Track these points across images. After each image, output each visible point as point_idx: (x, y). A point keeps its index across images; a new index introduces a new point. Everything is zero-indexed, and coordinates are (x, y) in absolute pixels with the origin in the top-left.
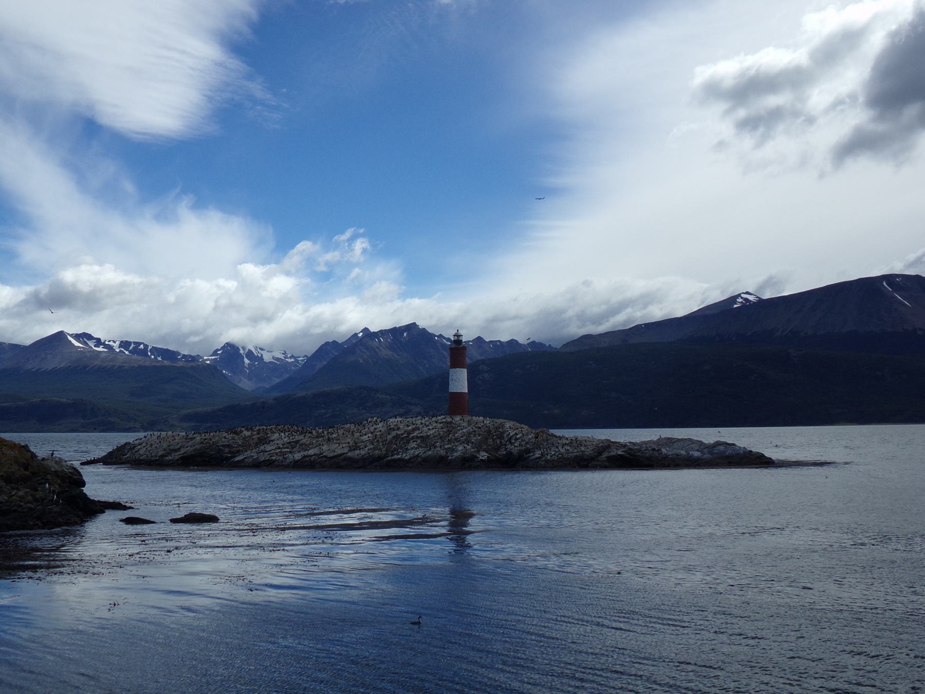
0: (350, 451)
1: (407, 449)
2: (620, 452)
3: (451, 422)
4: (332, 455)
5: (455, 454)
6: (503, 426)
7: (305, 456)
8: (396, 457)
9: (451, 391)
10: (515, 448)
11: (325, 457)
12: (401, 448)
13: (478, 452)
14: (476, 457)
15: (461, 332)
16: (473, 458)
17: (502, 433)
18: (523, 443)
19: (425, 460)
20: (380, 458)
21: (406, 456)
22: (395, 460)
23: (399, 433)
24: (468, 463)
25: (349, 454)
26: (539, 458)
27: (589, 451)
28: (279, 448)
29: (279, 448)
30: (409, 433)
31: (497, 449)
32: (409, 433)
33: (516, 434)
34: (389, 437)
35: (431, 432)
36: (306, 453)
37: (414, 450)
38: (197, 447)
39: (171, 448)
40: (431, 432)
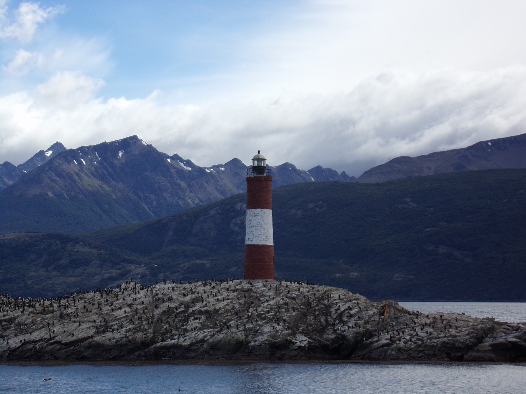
0: (98, 333)
1: (186, 331)
2: (511, 338)
3: (250, 290)
4: (70, 339)
5: (261, 339)
7: (25, 343)
8: (169, 342)
9: (248, 242)
10: (349, 330)
11: (59, 342)
12: (177, 329)
13: (294, 334)
14: (291, 342)
15: (263, 155)
16: (287, 344)
17: (328, 307)
18: (361, 322)
19: (215, 347)
20: (145, 344)
21: (185, 341)
22: (168, 348)
23: (172, 305)
24: (279, 353)
25: (97, 338)
26: (387, 345)
27: (463, 336)
30: (187, 307)
31: (322, 330)
33: (350, 308)
34: (157, 312)
35: (221, 305)
36: (27, 337)
40: (221, 305)
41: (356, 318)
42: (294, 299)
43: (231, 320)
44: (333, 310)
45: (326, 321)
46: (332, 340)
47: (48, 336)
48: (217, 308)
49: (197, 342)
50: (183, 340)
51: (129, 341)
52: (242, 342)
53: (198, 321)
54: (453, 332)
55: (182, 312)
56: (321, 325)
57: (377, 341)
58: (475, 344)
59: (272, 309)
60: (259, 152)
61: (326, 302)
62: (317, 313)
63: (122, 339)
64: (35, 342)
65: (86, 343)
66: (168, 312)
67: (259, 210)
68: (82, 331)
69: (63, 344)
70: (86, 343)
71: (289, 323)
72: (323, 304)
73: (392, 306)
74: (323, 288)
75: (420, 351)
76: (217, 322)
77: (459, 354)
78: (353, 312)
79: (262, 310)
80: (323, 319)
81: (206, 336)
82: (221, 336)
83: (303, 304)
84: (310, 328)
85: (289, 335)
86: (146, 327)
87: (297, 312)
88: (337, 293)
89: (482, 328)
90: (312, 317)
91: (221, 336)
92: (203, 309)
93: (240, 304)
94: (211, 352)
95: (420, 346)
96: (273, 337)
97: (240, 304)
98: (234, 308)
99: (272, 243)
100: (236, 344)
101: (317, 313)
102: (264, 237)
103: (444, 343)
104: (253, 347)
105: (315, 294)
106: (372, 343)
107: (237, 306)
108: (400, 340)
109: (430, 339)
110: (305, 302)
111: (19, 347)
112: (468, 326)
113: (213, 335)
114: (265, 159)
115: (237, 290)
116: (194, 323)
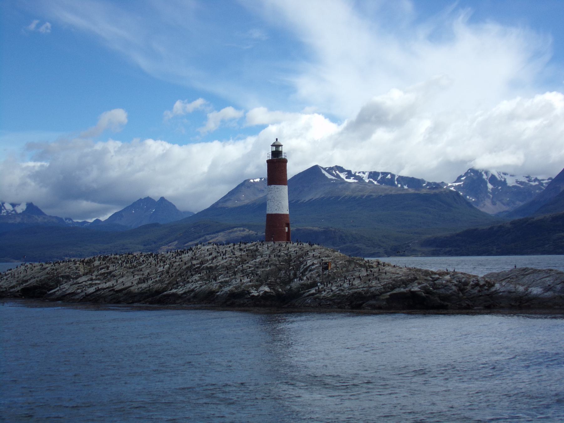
1: (188, 282)
6: (307, 253)
7: (98, 290)
8: (174, 291)
9: (269, 212)
11: (113, 290)
14: (249, 293)
17: (301, 263)
20: (158, 292)
21: (180, 291)
22: (168, 296)
26: (313, 294)
28: (92, 280)
29: (92, 280)
33: (313, 264)
34: (184, 267)
37: (196, 283)
38: (43, 278)
39: (24, 279)
43: (221, 274)
44: (302, 266)
49: (189, 292)
53: (199, 275)
54: (374, 283)
55: (197, 268)
56: (289, 278)
57: (309, 291)
58: (381, 293)
60: (277, 139)
61: (301, 259)
63: (146, 288)
64: (104, 289)
65: (124, 292)
67: (273, 186)
70: (124, 292)
71: (260, 277)
72: (300, 261)
73: (353, 261)
75: (331, 300)
76: (211, 276)
77: (361, 302)
78: (313, 267)
79: (247, 267)
81: (196, 287)
83: (285, 261)
84: (278, 280)
85: (252, 286)
87: (273, 267)
89: (402, 280)
90: (284, 272)
93: (236, 261)
96: (236, 288)
97: (236, 261)
98: (231, 264)
100: (208, 293)
102: (276, 207)
103: (356, 293)
104: (218, 296)
105: (296, 253)
106: (304, 293)
108: (325, 291)
109: (350, 289)
113: (201, 286)
115: (247, 250)
116: (196, 277)
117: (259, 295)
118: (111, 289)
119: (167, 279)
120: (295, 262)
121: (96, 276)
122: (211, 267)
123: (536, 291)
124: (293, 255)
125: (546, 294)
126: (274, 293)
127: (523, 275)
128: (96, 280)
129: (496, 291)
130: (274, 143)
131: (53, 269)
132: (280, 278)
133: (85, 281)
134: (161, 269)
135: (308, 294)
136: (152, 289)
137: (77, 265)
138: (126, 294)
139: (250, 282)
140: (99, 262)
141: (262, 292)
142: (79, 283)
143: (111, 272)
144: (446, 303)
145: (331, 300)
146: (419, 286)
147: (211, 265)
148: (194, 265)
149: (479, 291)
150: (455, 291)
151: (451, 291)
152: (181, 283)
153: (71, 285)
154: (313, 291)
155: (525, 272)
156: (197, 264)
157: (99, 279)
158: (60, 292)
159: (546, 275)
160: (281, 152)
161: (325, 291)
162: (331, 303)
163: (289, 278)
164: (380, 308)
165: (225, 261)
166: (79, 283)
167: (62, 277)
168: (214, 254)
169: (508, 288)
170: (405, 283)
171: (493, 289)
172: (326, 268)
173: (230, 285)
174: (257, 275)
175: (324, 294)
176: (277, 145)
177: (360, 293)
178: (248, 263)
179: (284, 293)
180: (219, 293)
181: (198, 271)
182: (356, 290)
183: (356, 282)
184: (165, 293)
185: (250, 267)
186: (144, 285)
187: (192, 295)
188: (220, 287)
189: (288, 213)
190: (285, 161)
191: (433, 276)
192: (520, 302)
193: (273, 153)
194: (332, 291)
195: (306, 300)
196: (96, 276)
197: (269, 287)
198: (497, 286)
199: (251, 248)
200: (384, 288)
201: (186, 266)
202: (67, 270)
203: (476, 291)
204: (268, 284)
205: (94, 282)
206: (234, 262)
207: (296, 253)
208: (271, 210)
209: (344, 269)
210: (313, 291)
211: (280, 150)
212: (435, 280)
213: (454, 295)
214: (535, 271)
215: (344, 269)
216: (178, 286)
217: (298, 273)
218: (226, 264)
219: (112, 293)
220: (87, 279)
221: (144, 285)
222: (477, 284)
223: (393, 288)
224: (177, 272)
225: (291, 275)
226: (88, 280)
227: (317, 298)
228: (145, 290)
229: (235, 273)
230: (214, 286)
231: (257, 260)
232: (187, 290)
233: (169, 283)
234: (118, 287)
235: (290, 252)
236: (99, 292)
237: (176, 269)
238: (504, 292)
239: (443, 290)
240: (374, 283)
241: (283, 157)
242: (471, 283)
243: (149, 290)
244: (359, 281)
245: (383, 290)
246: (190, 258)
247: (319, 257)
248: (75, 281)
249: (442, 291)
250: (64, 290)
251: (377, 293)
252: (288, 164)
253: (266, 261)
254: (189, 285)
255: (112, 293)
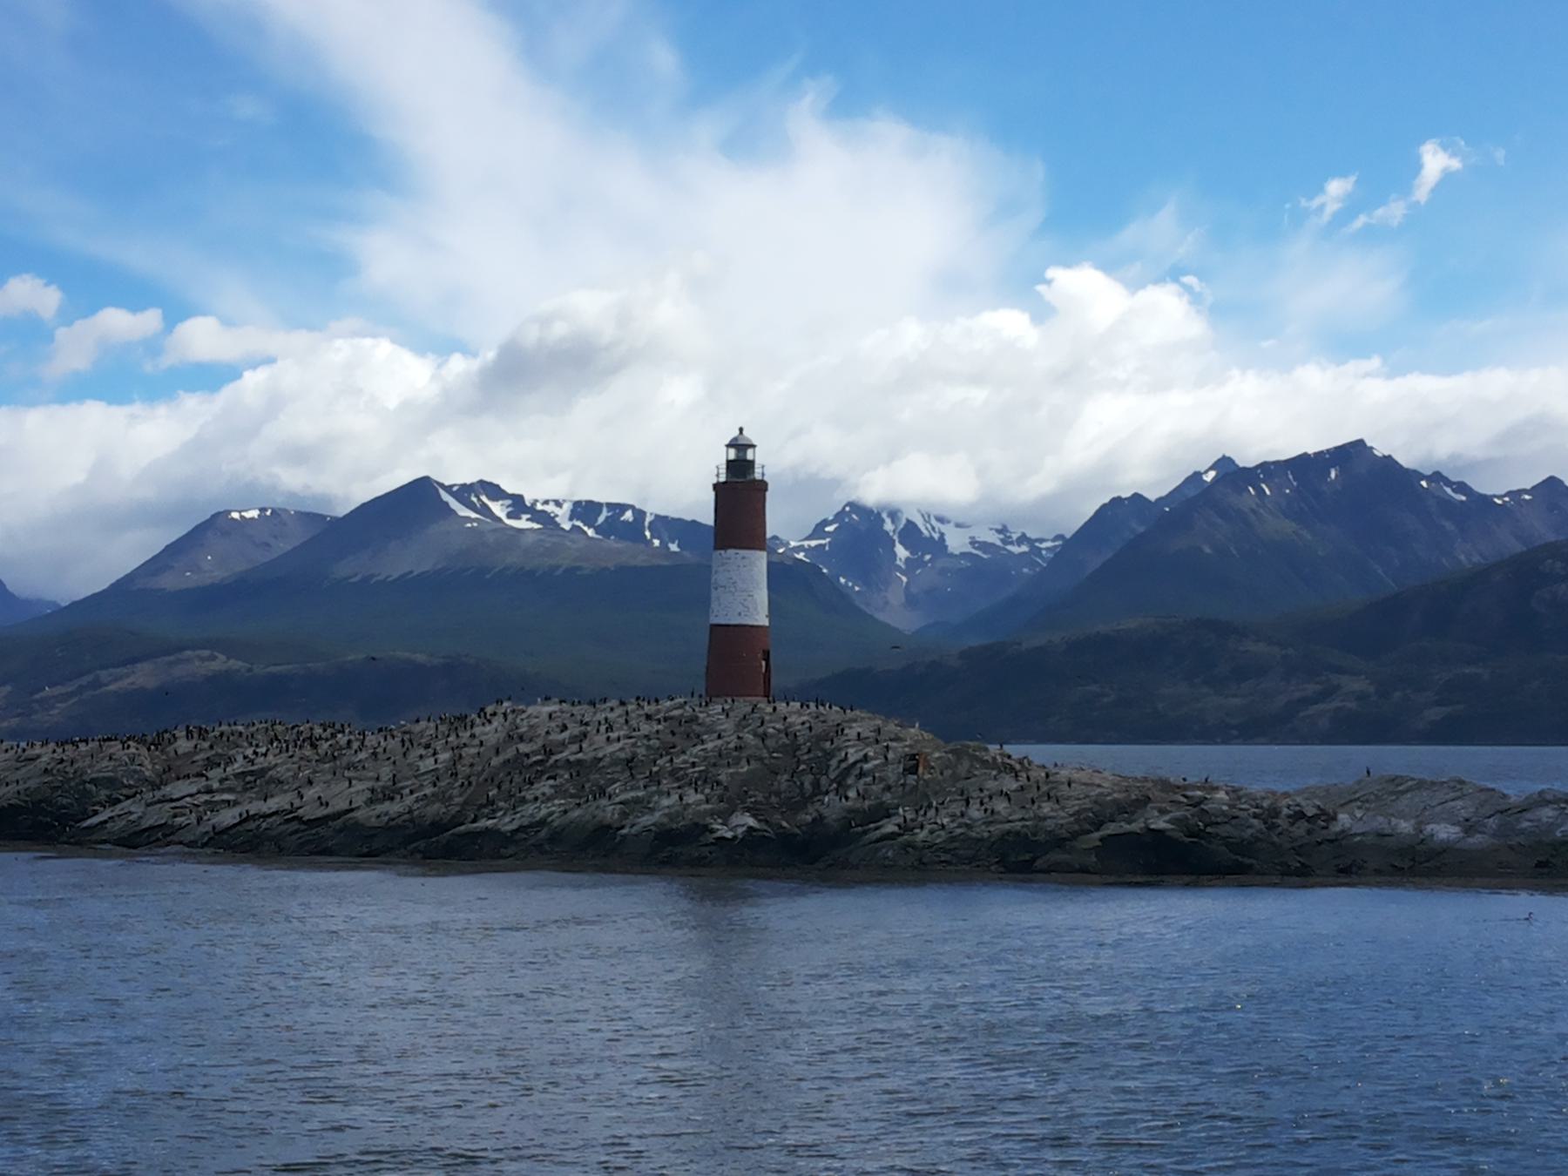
1: (523, 801)
2: (1160, 824)
3: (693, 719)
5: (647, 820)
7: (249, 818)
17: (829, 755)
19: (556, 836)
20: (438, 827)
21: (507, 823)
23: (524, 748)
26: (892, 836)
28: (209, 791)
29: (209, 791)
31: (795, 805)
32: (548, 751)
33: (866, 759)
34: (495, 761)
35: (610, 749)
37: (545, 803)
38: (32, 784)
40: (610, 749)
41: (869, 779)
42: (763, 737)
44: (834, 762)
45: (816, 784)
46: (807, 824)
47: (288, 807)
48: (600, 755)
49: (531, 826)
50: (507, 819)
51: (412, 821)
52: (609, 827)
53: (551, 782)
54: (1046, 808)
55: (536, 763)
56: (802, 794)
57: (877, 828)
58: (1075, 835)
59: (705, 758)
60: (741, 430)
62: (802, 767)
64: (265, 816)
66: (518, 761)
67: (731, 552)
68: (340, 794)
69: (304, 823)
71: (726, 788)
72: (823, 750)
74: (834, 714)
76: (587, 786)
77: (1027, 857)
78: (867, 766)
79: (685, 762)
80: (808, 780)
81: (551, 814)
82: (577, 813)
83: (782, 748)
85: (712, 813)
86: (455, 792)
87: (754, 765)
88: (862, 724)
89: (1115, 800)
90: (786, 777)
91: (577, 813)
92: (572, 758)
93: (648, 747)
94: (547, 847)
95: (953, 839)
97: (648, 747)
99: (766, 622)
101: (802, 767)
102: (740, 608)
103: (1009, 832)
104: (624, 836)
105: (810, 728)
106: (865, 833)
107: (642, 751)
108: (922, 827)
110: (785, 745)
111: (235, 825)
112: (1087, 796)
113: (565, 812)
114: (753, 446)
115: (666, 719)
116: (544, 787)
117: (735, 837)
118: (290, 815)
119: (455, 792)
120: (809, 751)
121: (221, 781)
122: (579, 762)
123: (1444, 832)
124: (803, 735)
125: (1471, 840)
126: (771, 834)
127: (1392, 793)
128: (223, 791)
129: (1343, 831)
130: (735, 439)
131: (62, 761)
132: (778, 794)
133: (191, 795)
134: (429, 764)
135: (878, 833)
136: (420, 817)
137: (132, 750)
138: (341, 831)
139: (707, 801)
140: (194, 742)
141: (740, 830)
142: (172, 800)
143: (263, 771)
144: (1247, 861)
145: (946, 851)
146: (1167, 817)
147: (580, 756)
148: (527, 756)
149: (1309, 832)
150: (1260, 831)
151: (1250, 831)
152: (501, 804)
153: (148, 805)
154: (889, 827)
155: (1396, 785)
156: (535, 753)
157: (230, 790)
158: (122, 823)
159: (1452, 795)
160: (752, 463)
161: (922, 827)
162: (946, 857)
163: (802, 794)
164: (1084, 870)
165: (617, 746)
166: (172, 800)
167: (92, 781)
168: (575, 729)
169: (1375, 825)
170: (1129, 808)
171: (1336, 828)
172: (913, 770)
173: (652, 810)
174: (718, 783)
175: (922, 835)
176: (740, 445)
177: (1018, 833)
178: (684, 752)
179: (797, 831)
180: (624, 831)
181: (542, 769)
182: (1007, 826)
183: (1001, 806)
184: (462, 828)
185: (694, 765)
186: (394, 808)
187: (543, 833)
188: (624, 815)
189: (766, 622)
190: (762, 486)
191: (1189, 793)
192: (1413, 860)
193: (730, 464)
194: (943, 826)
195: (878, 850)
196: (221, 781)
197: (754, 816)
198: (1344, 819)
199: (676, 713)
200: (1077, 821)
201: (501, 758)
202: (105, 763)
203: (1301, 828)
204: (748, 810)
205: (218, 798)
206: (642, 751)
207: (810, 728)
208: (725, 612)
209: (948, 773)
210: (889, 827)
211: (750, 455)
212: (1197, 803)
213: (1258, 839)
214: (1421, 785)
215: (948, 773)
216: (494, 811)
217: (824, 780)
218: (622, 755)
219: (295, 826)
220: (194, 790)
221: (394, 808)
222: (1300, 815)
223: (1098, 826)
224: (479, 775)
225: (807, 785)
226: (199, 792)
227: (910, 845)
228: (399, 821)
229: (654, 779)
230: (608, 811)
231: (710, 746)
232: (526, 822)
233: (466, 803)
234: (310, 812)
235: (791, 725)
236: (252, 825)
237: (472, 765)
238: (1363, 834)
239: (1228, 827)
240: (1046, 808)
241: (758, 476)
242: (1285, 811)
243: (412, 821)
244: (1005, 804)
245: (1076, 827)
246: (502, 735)
247: (877, 742)
248: (158, 794)
249: (1224, 830)
250: (132, 818)
251: (1066, 835)
252: (768, 494)
253: (736, 749)
254: (530, 809)
255: (295, 826)
